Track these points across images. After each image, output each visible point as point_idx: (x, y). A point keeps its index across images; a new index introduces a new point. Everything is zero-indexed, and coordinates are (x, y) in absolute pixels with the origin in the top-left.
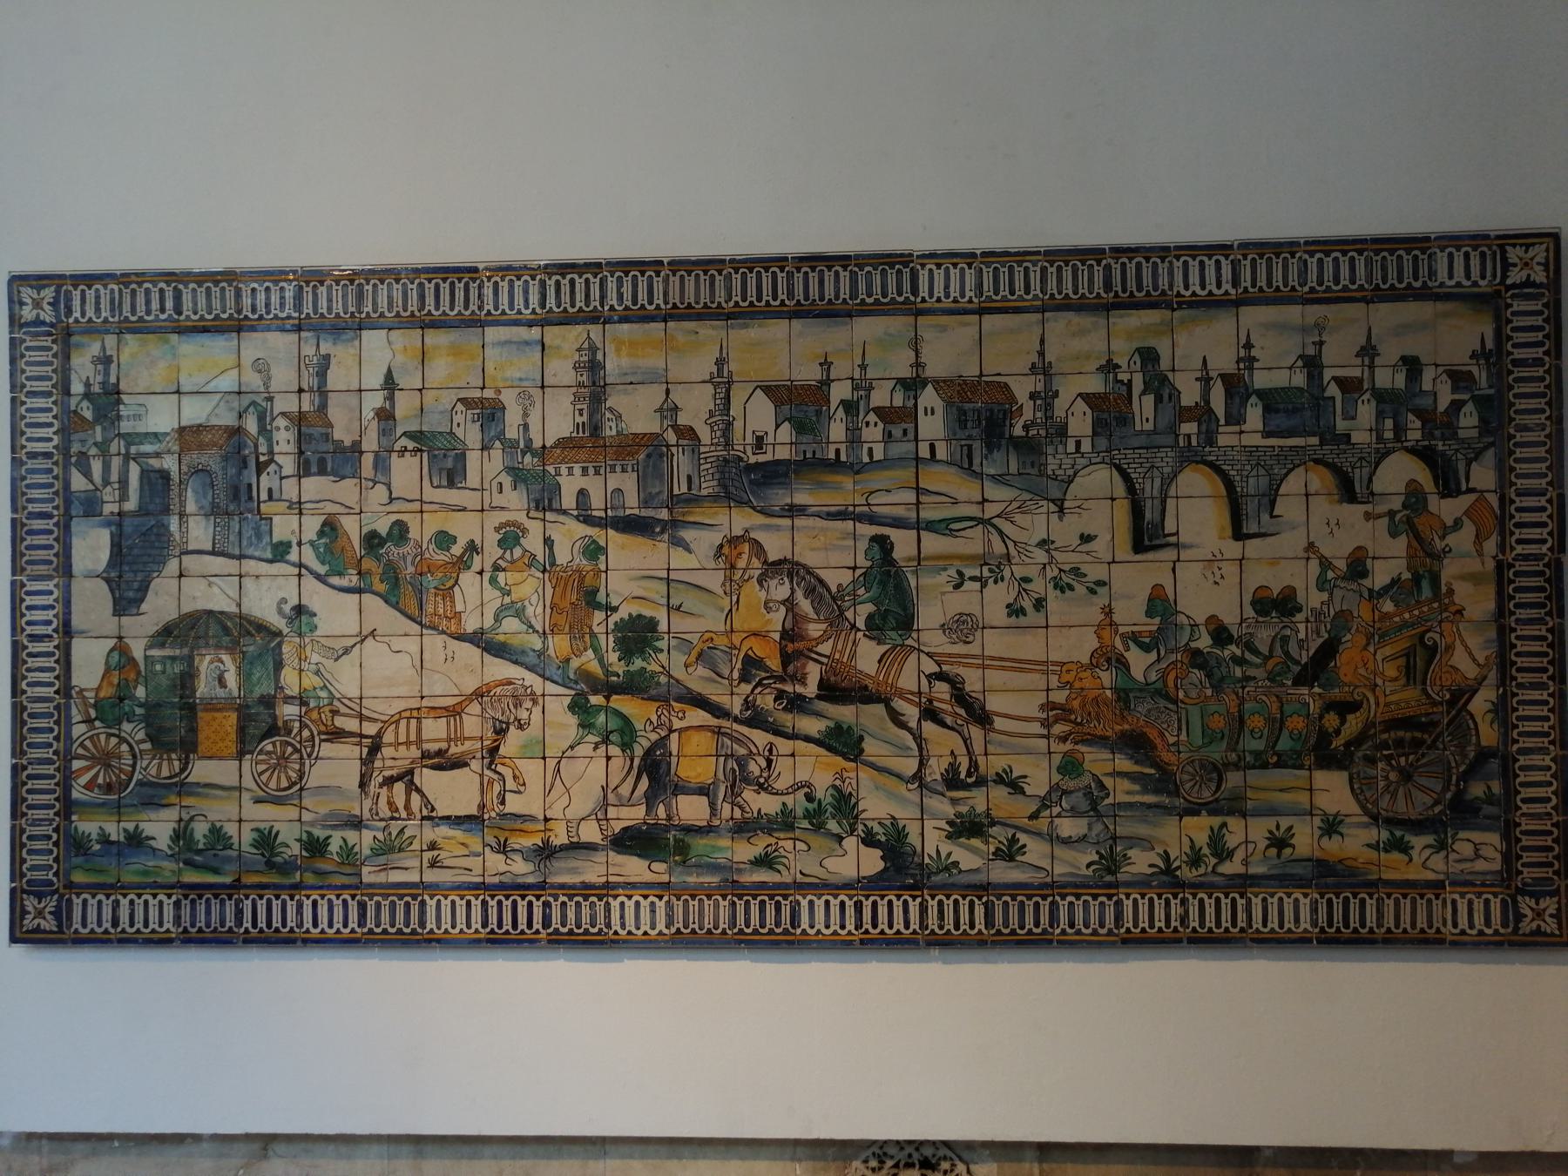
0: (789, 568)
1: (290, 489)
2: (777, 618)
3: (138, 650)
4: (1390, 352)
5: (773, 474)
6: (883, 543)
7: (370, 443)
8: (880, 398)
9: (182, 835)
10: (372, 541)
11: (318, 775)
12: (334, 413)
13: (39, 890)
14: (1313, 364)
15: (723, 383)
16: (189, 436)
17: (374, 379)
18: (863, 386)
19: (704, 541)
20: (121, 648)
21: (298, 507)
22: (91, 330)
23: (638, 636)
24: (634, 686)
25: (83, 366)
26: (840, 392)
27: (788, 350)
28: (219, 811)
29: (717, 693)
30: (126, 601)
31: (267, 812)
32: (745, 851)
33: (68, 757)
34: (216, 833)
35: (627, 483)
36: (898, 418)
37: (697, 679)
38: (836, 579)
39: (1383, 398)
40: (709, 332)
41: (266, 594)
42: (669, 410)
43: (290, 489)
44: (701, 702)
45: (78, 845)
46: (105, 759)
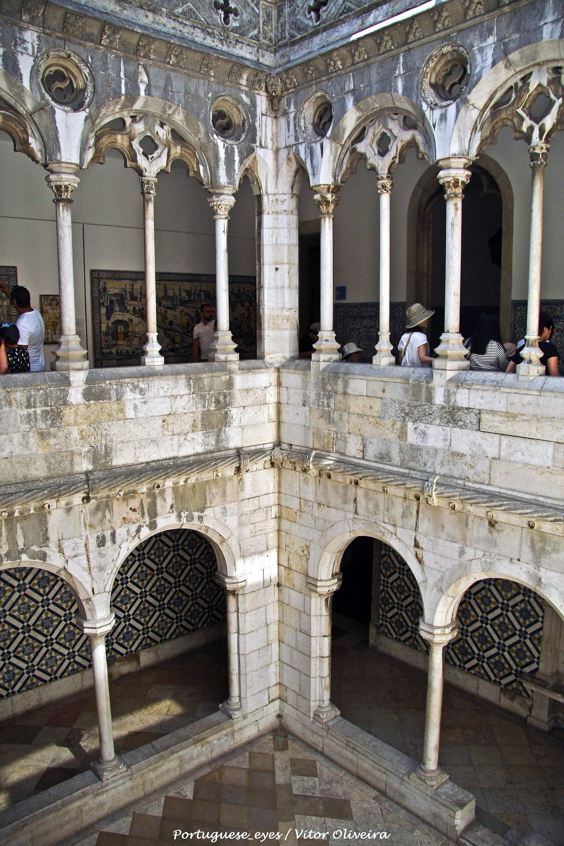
0: (187, 314)
1: (129, 303)
2: (186, 321)
3: (110, 325)
4: (247, 289)
5: (186, 302)
6: (197, 311)
7: (139, 297)
8: (197, 292)
9: (117, 351)
10: (140, 310)
11: (134, 342)
12: (135, 292)
13: (98, 360)
14: (239, 290)
15: (180, 290)
16: (115, 295)
17: (139, 287)
18: (195, 291)
19: (178, 310)
20: (108, 325)
21: (130, 305)
22: (103, 278)
23: (171, 323)
24: (171, 330)
25: (101, 284)
26: (193, 291)
27: (187, 286)
28: (121, 348)
29: (180, 330)
30: (108, 318)
31: (127, 348)
32: (183, 351)
33: (101, 341)
34: (121, 351)
35: (170, 302)
36: (199, 295)
37: (178, 329)
38: (193, 315)
39: (246, 295)
40: (179, 283)
41: (126, 317)
42: (174, 293)
43: (129, 303)
44: (178, 332)
45: (103, 353)
46: (106, 341)
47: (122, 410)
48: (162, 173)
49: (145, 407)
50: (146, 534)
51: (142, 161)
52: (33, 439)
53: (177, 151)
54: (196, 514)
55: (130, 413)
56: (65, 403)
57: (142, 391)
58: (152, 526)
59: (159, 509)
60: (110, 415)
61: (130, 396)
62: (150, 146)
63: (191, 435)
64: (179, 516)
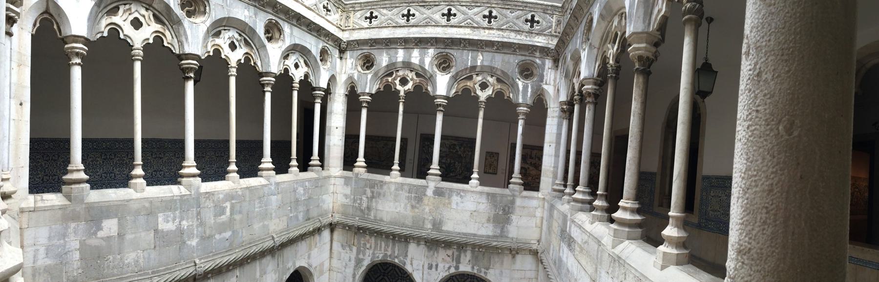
47: (450, 203)
48: (489, 99)
49: (462, 205)
50: (453, 270)
51: (479, 92)
52: (409, 207)
53: (499, 86)
54: (483, 270)
55: (454, 206)
56: (425, 195)
57: (461, 196)
58: (457, 268)
59: (462, 260)
60: (444, 204)
61: (455, 199)
62: (484, 86)
63: (486, 225)
64: (473, 268)
